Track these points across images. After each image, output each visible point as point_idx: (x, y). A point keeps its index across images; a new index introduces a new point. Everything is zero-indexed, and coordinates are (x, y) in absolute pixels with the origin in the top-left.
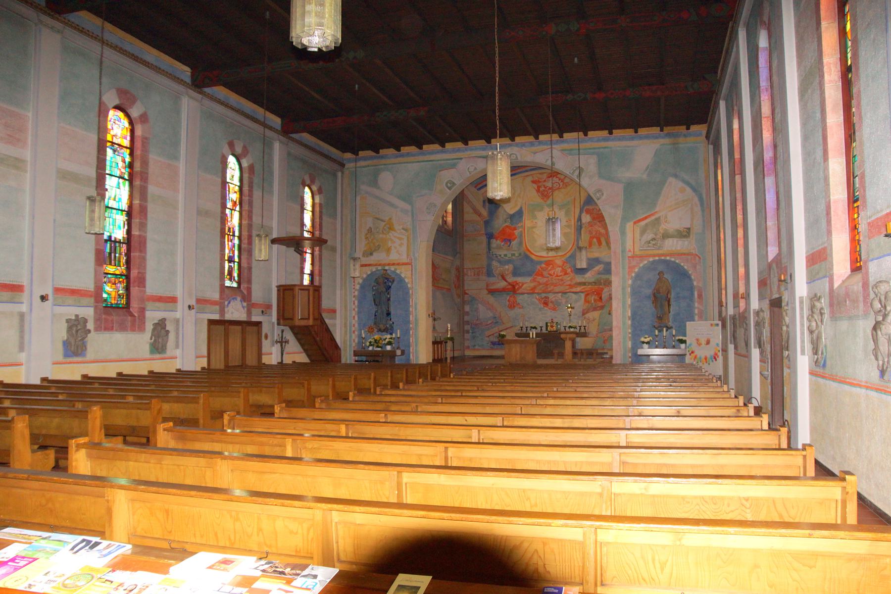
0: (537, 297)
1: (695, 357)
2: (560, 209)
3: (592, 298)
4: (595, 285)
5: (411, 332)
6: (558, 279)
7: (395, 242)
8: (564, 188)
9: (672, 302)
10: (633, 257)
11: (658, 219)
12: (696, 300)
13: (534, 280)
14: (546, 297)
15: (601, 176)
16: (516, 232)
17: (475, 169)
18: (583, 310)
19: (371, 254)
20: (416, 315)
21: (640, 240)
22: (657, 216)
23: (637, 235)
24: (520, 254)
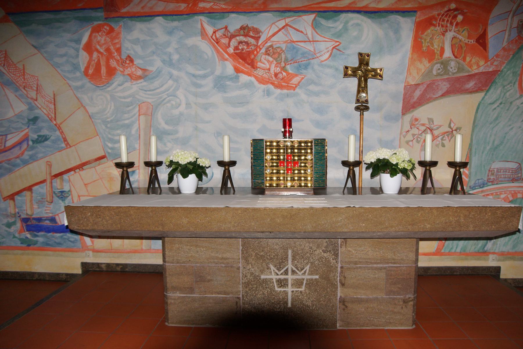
0: (210, 30)
14: (245, 30)
18: (409, 89)
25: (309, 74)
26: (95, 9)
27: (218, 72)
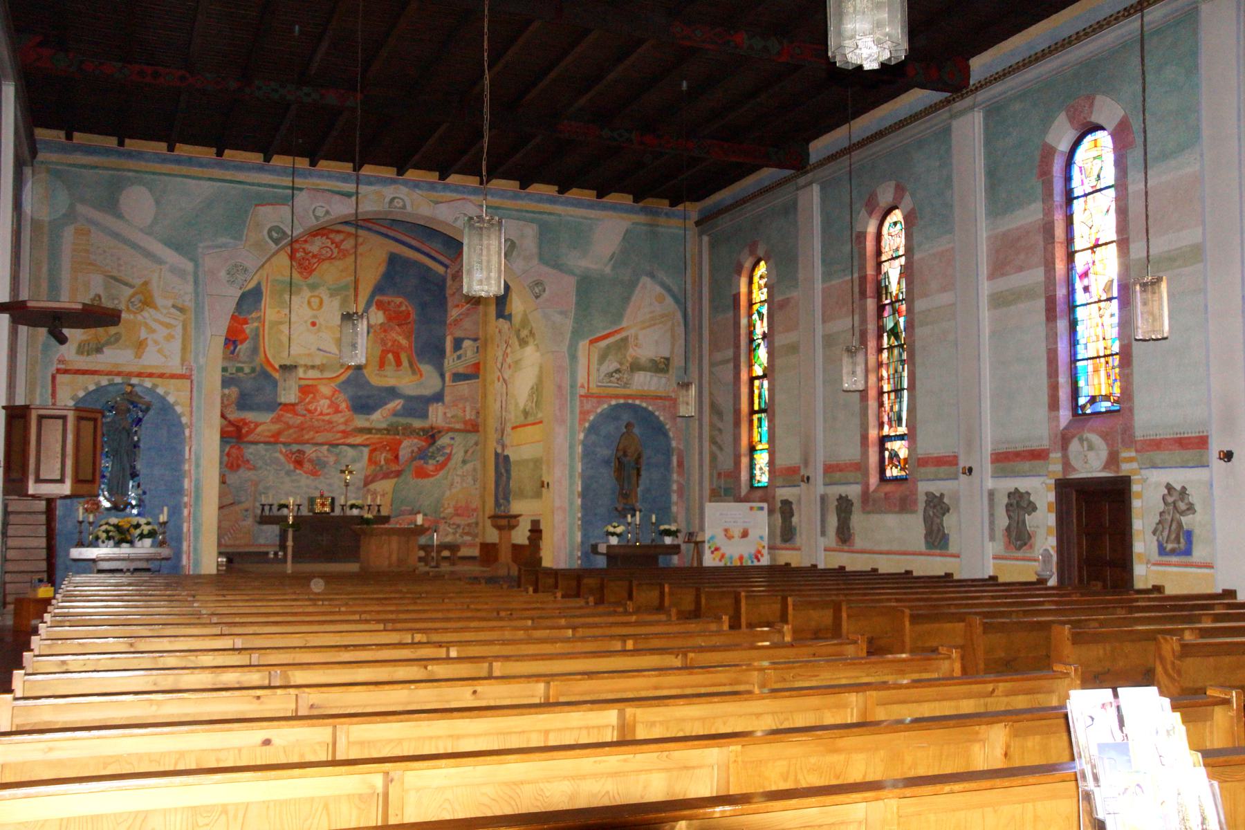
0: (284, 450)
1: (723, 556)
2: (331, 296)
3: (382, 457)
4: (388, 434)
5: (186, 512)
6: (323, 420)
7: (153, 331)
8: (340, 259)
9: (643, 473)
10: (586, 396)
11: (625, 340)
12: (675, 470)
13: (278, 420)
14: (299, 451)
15: (542, 259)
16: (248, 329)
17: (327, 212)
18: (366, 477)
19: (99, 350)
20: (198, 480)
21: (598, 370)
22: (624, 334)
23: (594, 365)
24: (253, 370)
25: (326, 470)
26: (232, 437)
27: (287, 468)
